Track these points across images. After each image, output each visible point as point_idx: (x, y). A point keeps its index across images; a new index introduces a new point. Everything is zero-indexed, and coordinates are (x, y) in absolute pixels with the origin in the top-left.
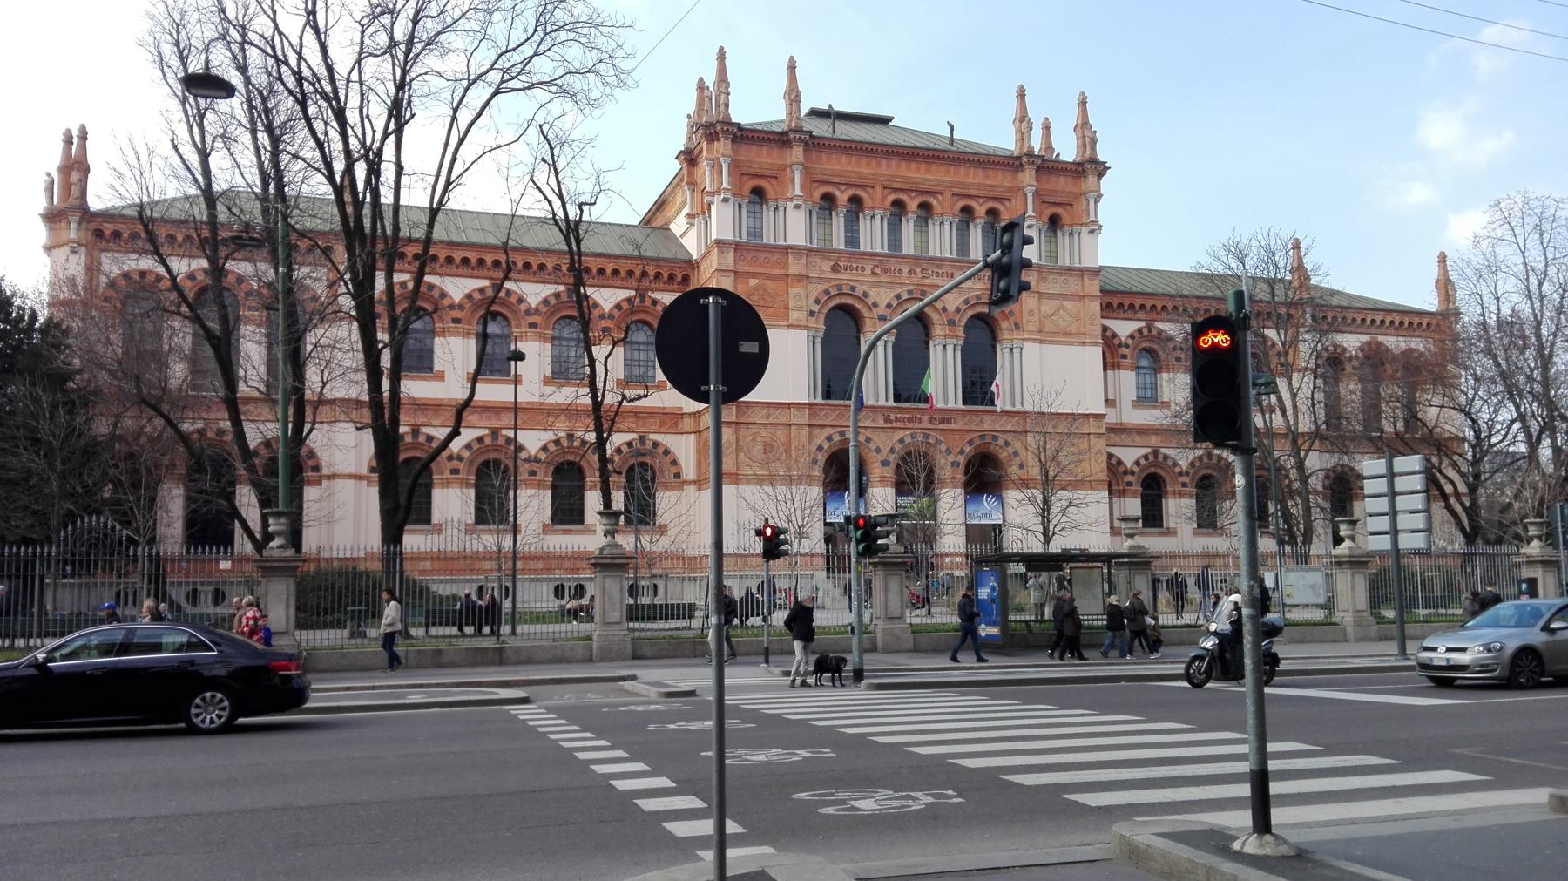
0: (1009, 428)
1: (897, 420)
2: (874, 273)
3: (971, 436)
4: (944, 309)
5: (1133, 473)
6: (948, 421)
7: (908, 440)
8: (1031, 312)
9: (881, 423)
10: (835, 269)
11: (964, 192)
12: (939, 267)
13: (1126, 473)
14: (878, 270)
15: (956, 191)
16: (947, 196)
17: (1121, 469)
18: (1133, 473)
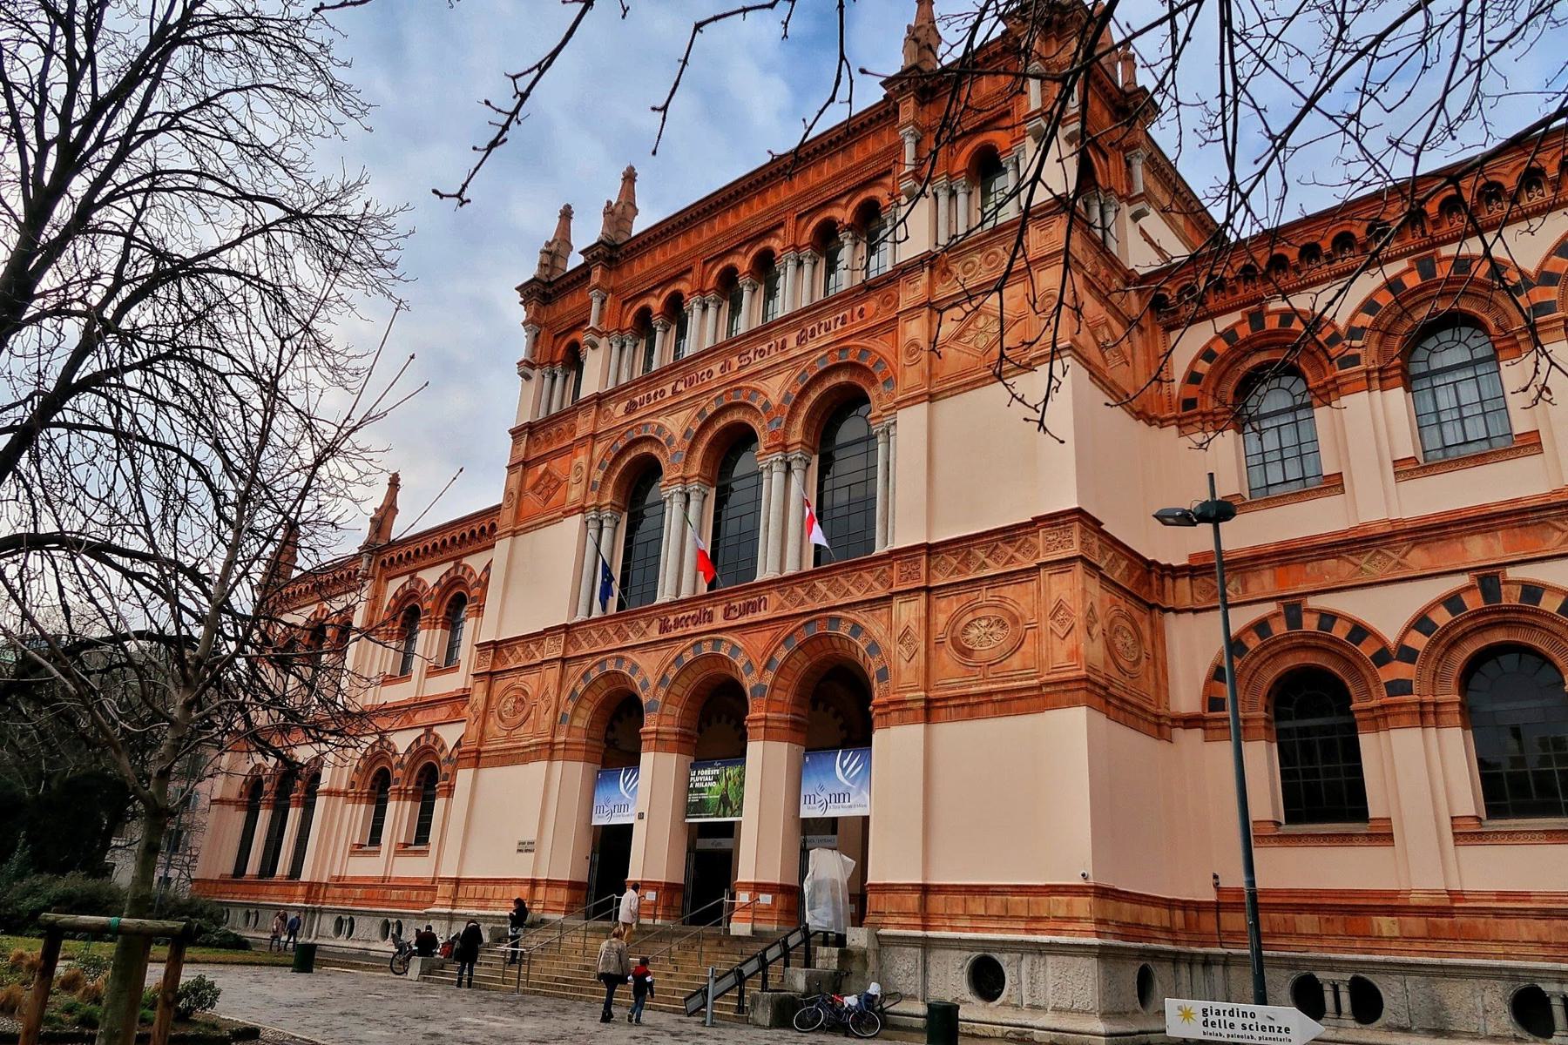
0: (858, 596)
1: (678, 623)
2: (675, 392)
3: (791, 627)
4: (766, 406)
5: (1408, 655)
6: (754, 607)
7: (689, 657)
8: (914, 345)
9: (654, 634)
10: (629, 411)
11: (816, 201)
12: (766, 339)
13: (1383, 657)
14: (681, 387)
15: (803, 208)
16: (790, 224)
17: (1366, 650)
18: (1408, 655)
